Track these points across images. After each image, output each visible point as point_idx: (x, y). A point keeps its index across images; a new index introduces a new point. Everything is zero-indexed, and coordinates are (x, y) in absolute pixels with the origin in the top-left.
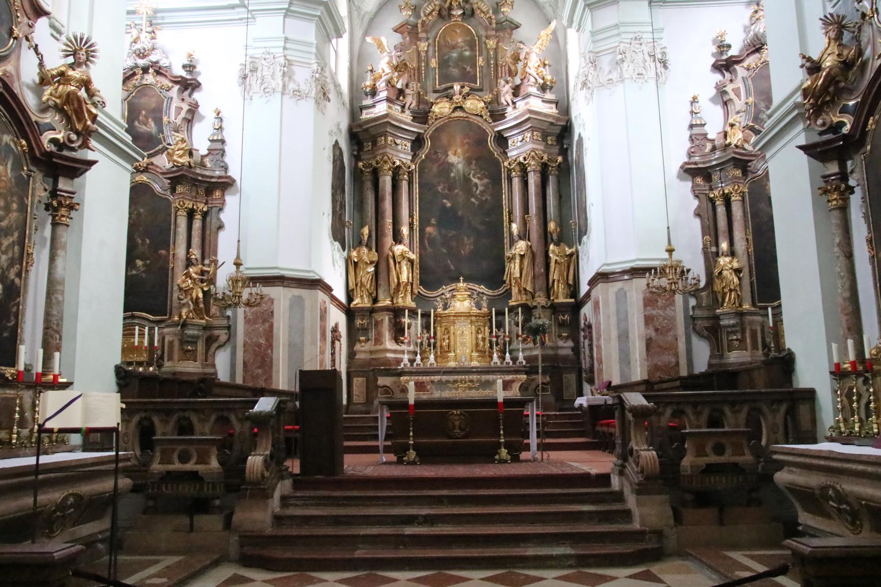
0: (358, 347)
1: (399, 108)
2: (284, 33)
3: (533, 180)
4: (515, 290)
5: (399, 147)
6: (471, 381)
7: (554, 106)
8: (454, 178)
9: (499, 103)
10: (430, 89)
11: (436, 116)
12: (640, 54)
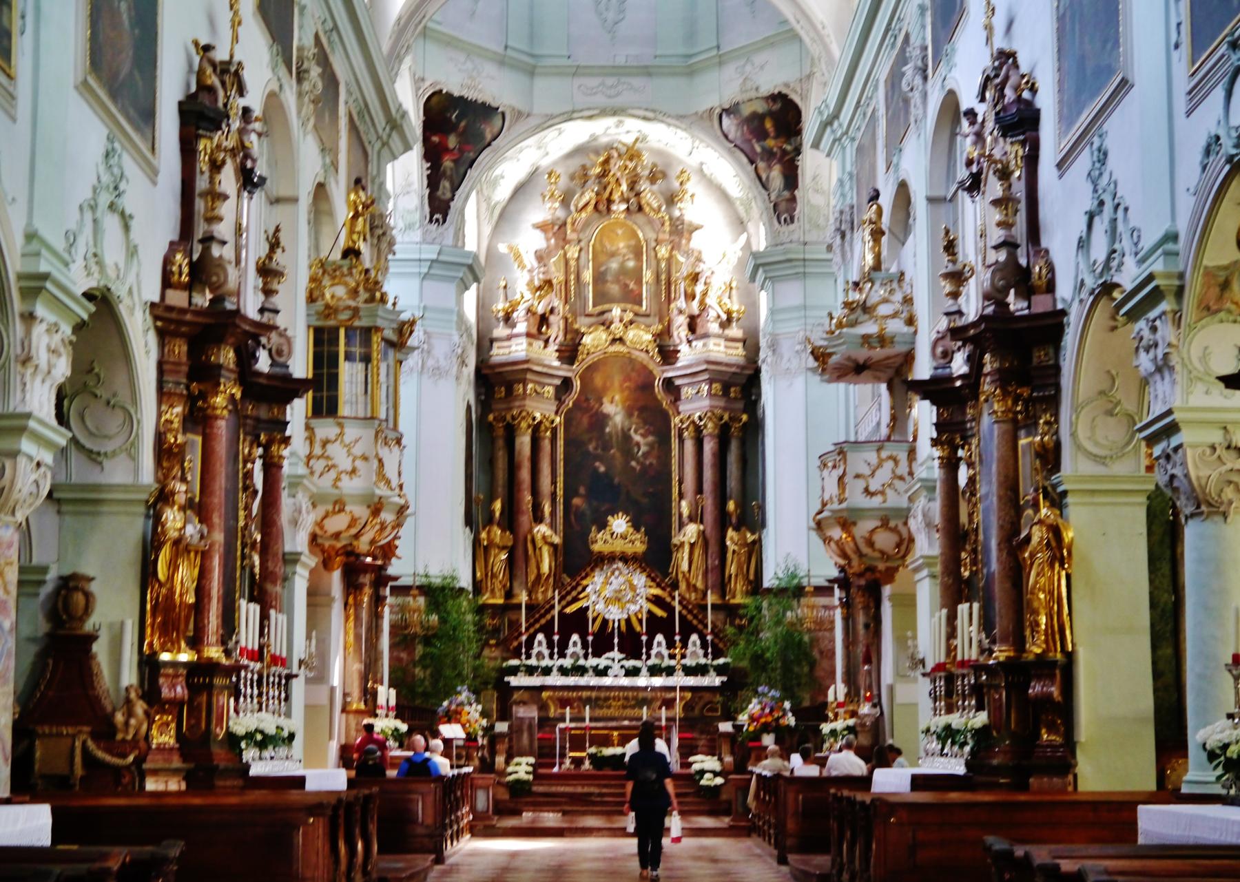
0: (486, 652)
1: (542, 344)
2: (421, 300)
3: (709, 447)
6: (626, 698)
7: (740, 345)
8: (610, 433)
9: (670, 336)
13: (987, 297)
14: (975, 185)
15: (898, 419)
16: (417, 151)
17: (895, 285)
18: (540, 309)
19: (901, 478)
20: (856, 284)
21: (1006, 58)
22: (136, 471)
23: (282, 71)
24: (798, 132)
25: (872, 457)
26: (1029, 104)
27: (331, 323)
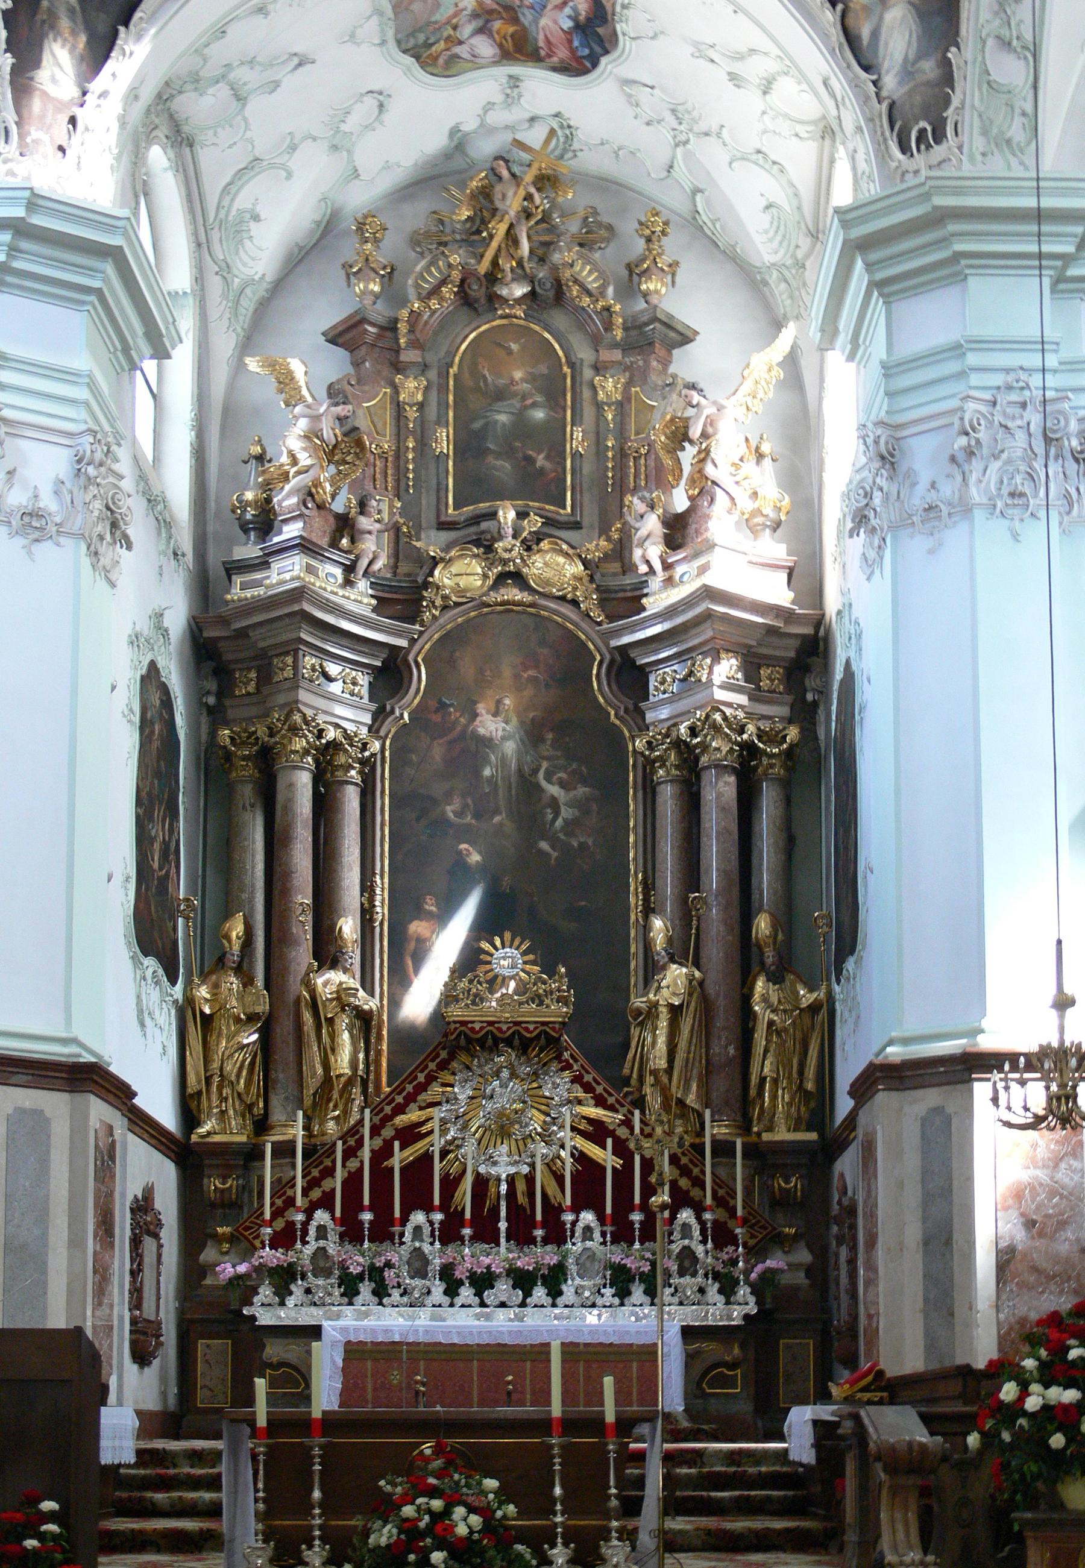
1: (338, 572)
5: (336, 688)
9: (628, 567)
11: (445, 598)
12: (1021, 436)
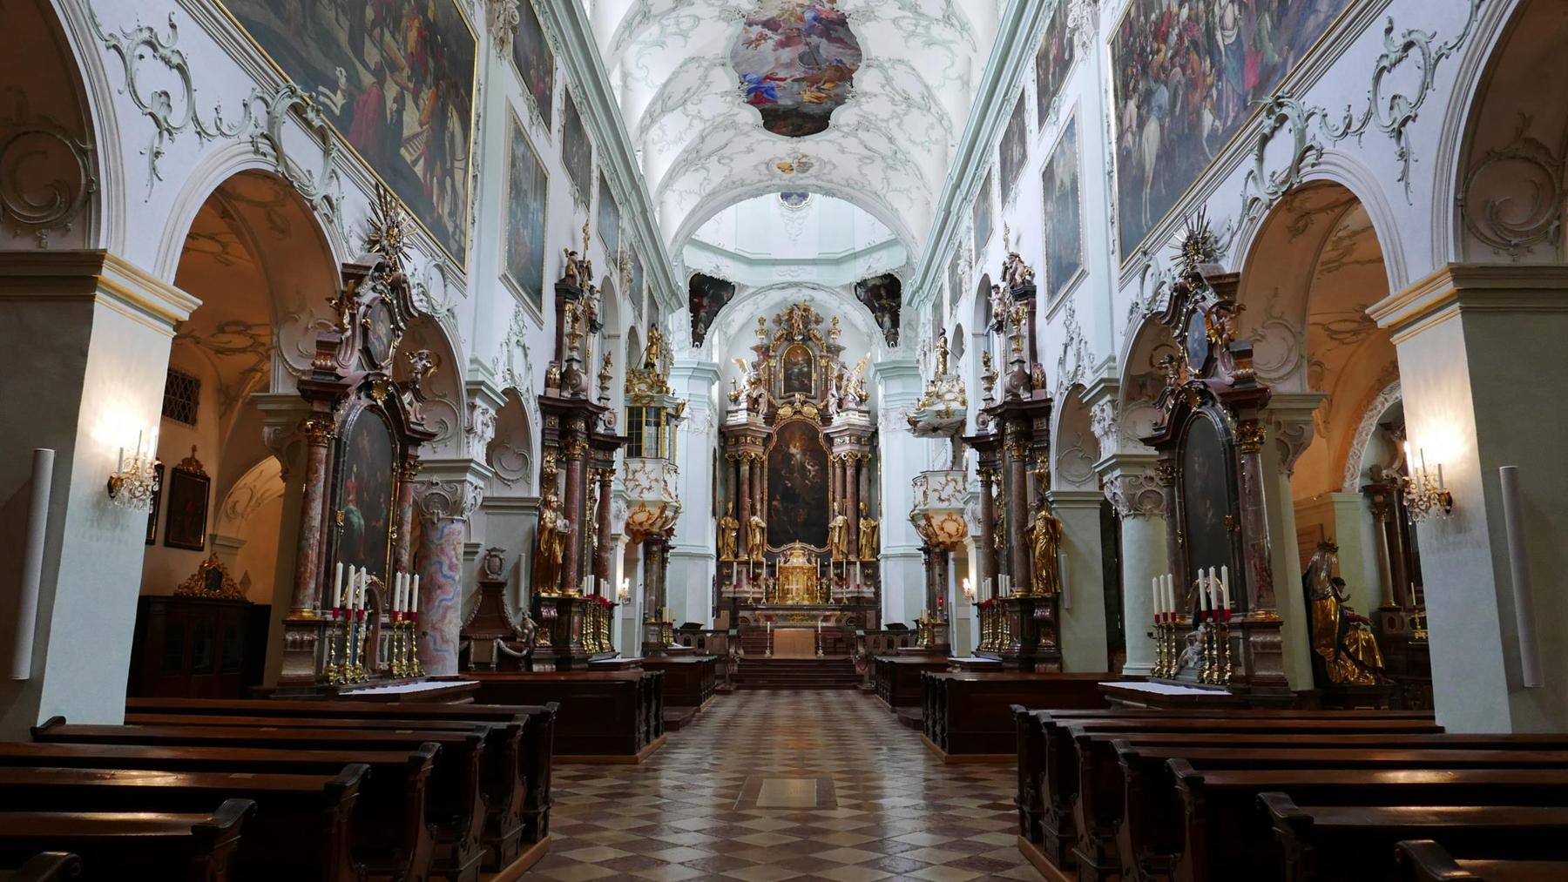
0: (724, 589)
4: (834, 552)
6: (803, 615)
10: (777, 395)
13: (1007, 391)
14: (999, 328)
15: (957, 458)
16: (686, 306)
17: (955, 383)
18: (754, 395)
19: (959, 491)
20: (933, 382)
21: (1014, 257)
22: (530, 490)
23: (612, 266)
24: (899, 296)
25: (943, 480)
26: (1029, 282)
27: (639, 405)
